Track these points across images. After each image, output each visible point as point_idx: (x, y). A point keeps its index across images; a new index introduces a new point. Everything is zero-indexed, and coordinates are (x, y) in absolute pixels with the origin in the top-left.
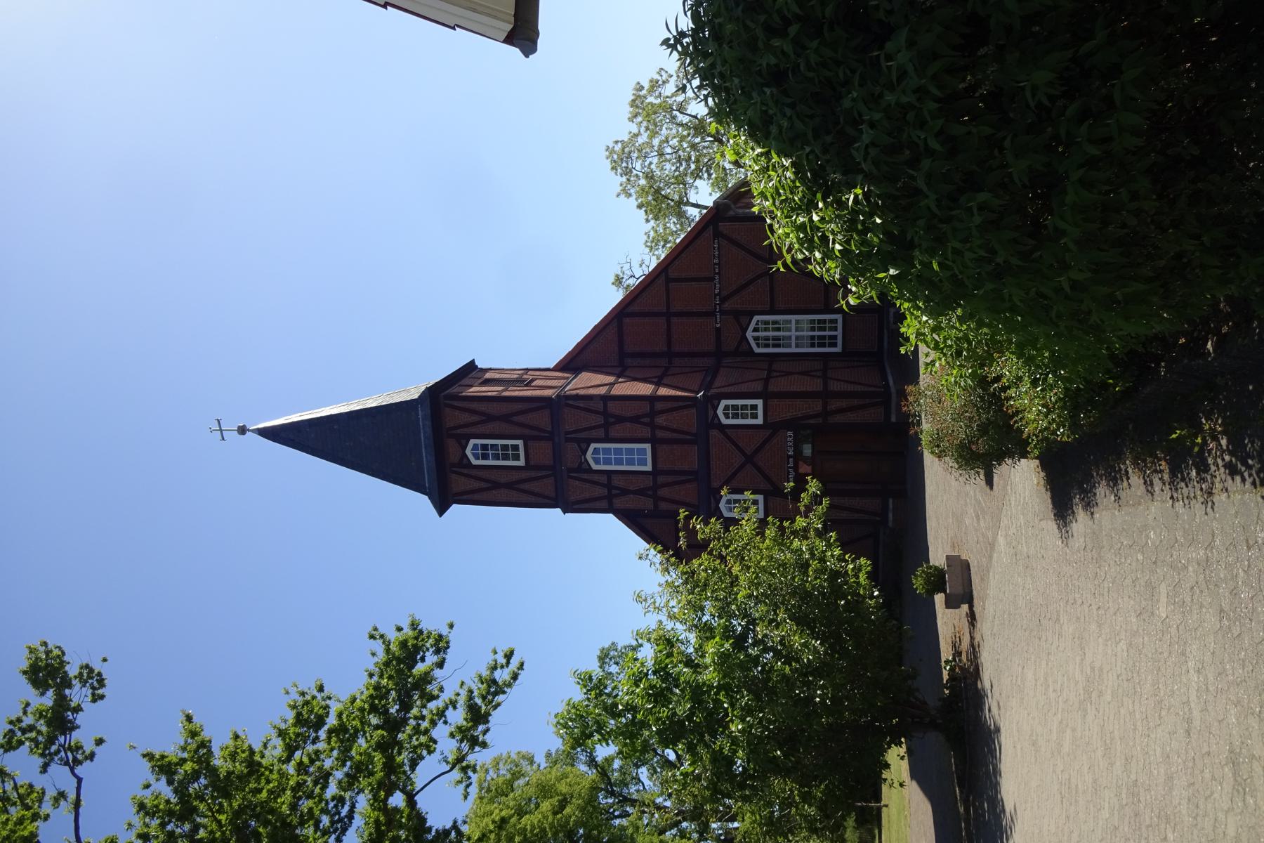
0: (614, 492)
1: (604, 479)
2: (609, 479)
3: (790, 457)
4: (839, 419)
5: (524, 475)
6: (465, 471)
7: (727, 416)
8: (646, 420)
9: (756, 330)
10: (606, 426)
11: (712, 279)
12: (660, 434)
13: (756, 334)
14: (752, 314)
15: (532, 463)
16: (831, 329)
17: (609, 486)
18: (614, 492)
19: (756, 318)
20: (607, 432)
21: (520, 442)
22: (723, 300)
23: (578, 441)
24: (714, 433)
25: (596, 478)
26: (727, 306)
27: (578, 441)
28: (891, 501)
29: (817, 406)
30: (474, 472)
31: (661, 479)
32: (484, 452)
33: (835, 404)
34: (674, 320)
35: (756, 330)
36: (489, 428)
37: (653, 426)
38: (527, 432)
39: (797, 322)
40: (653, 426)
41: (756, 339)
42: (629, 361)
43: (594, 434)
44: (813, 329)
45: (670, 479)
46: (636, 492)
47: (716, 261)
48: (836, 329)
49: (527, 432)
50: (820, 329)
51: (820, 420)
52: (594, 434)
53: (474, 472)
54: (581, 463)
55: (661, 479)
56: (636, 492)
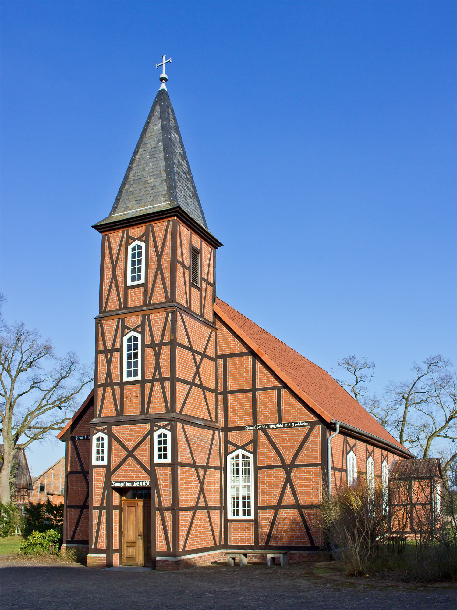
0: (109, 354)
1: (118, 346)
2: (117, 350)
3: (132, 483)
4: (158, 518)
5: (121, 286)
6: (124, 242)
7: (160, 436)
8: (157, 375)
9: (243, 456)
10: (153, 345)
11: (280, 422)
12: (148, 386)
13: (240, 457)
14: (255, 452)
15: (129, 291)
16: (244, 512)
17: (113, 350)
18: (109, 354)
19: (252, 456)
20: (149, 346)
21: (143, 281)
22: (264, 431)
23: (143, 325)
24: (148, 426)
25: (118, 340)
26: (261, 434)
27: (143, 325)
28: (105, 555)
29: (167, 502)
30: (123, 249)
31: (117, 388)
32: (136, 254)
33: (168, 515)
34: (250, 395)
35: (243, 456)
36: (153, 256)
37: (152, 381)
38: (150, 286)
39: (249, 487)
40: (152, 381)
41: (237, 457)
42: (220, 362)
43: (148, 336)
44: (244, 498)
45: (118, 396)
46: (109, 371)
47: (293, 425)
48: (244, 514)
49: (150, 286)
50: (244, 503)
51: (157, 506)
52: (148, 336)
53: (123, 249)
54: (129, 328)
55: (117, 388)
56: (109, 371)
